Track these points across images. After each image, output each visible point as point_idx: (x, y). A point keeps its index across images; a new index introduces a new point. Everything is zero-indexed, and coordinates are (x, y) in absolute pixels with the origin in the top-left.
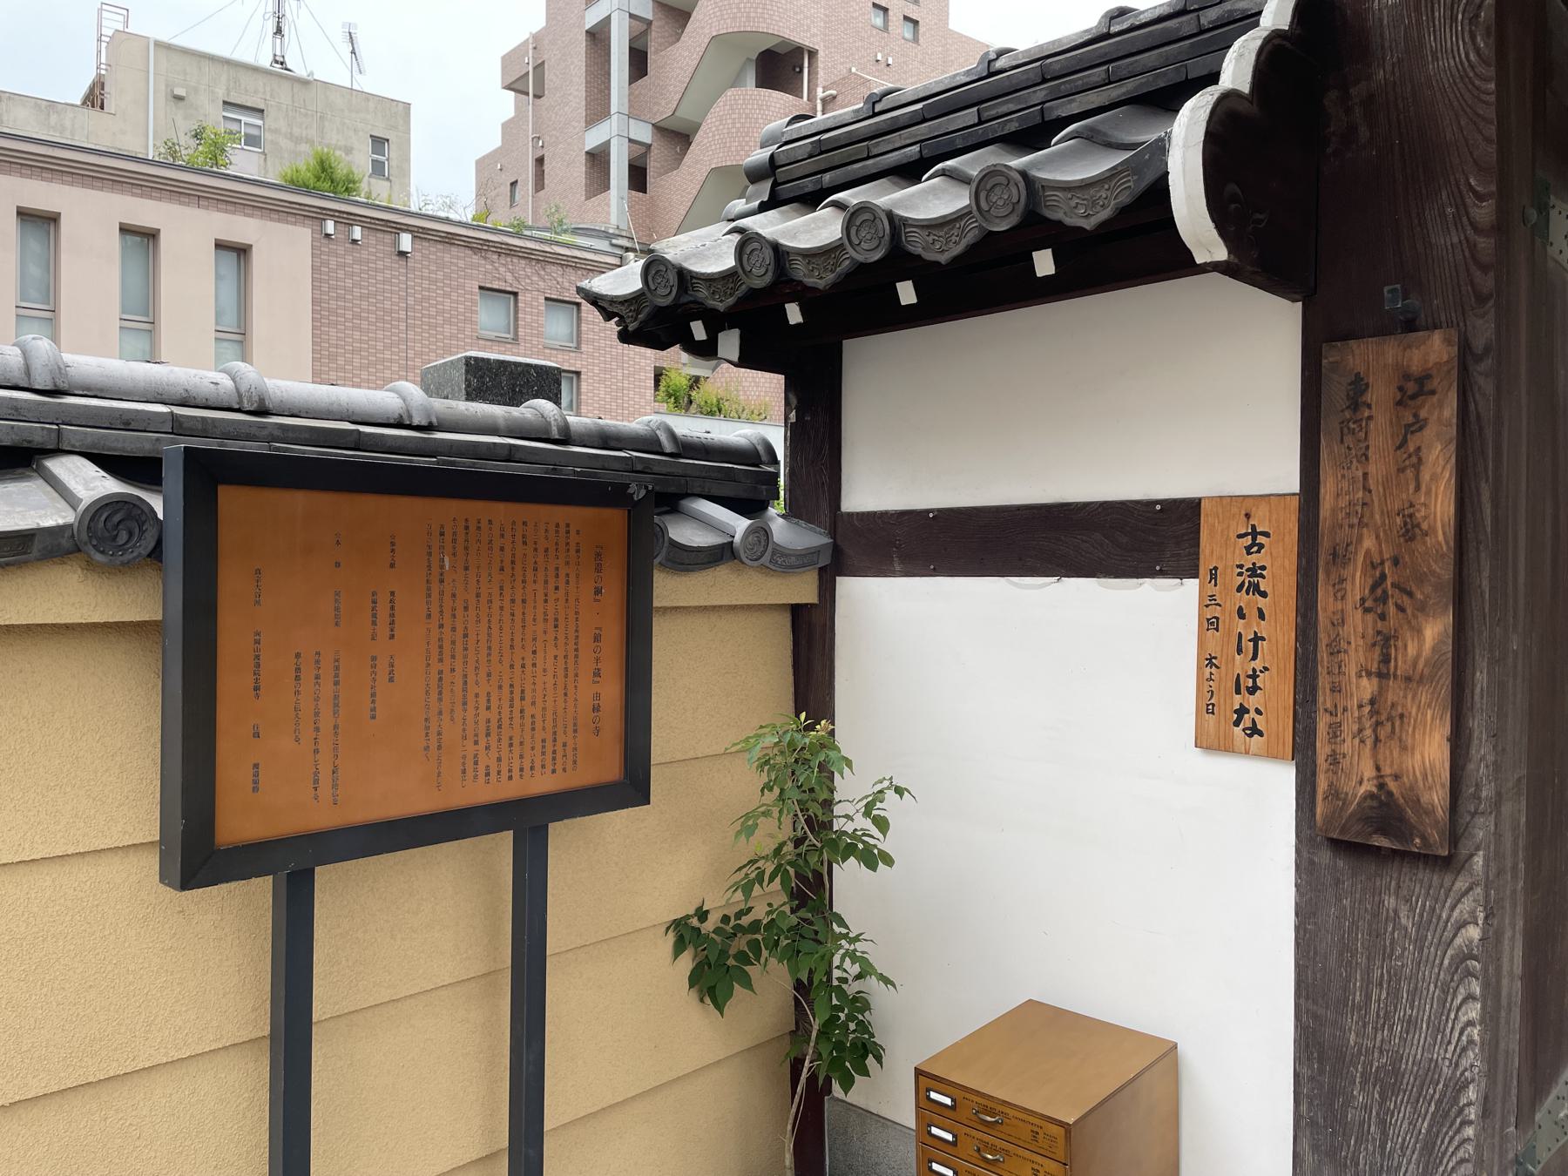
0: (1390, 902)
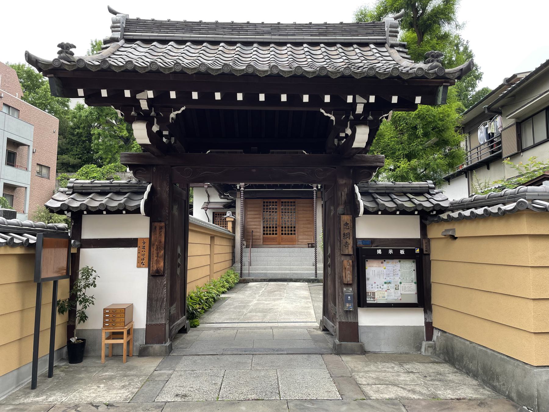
0: (157, 281)
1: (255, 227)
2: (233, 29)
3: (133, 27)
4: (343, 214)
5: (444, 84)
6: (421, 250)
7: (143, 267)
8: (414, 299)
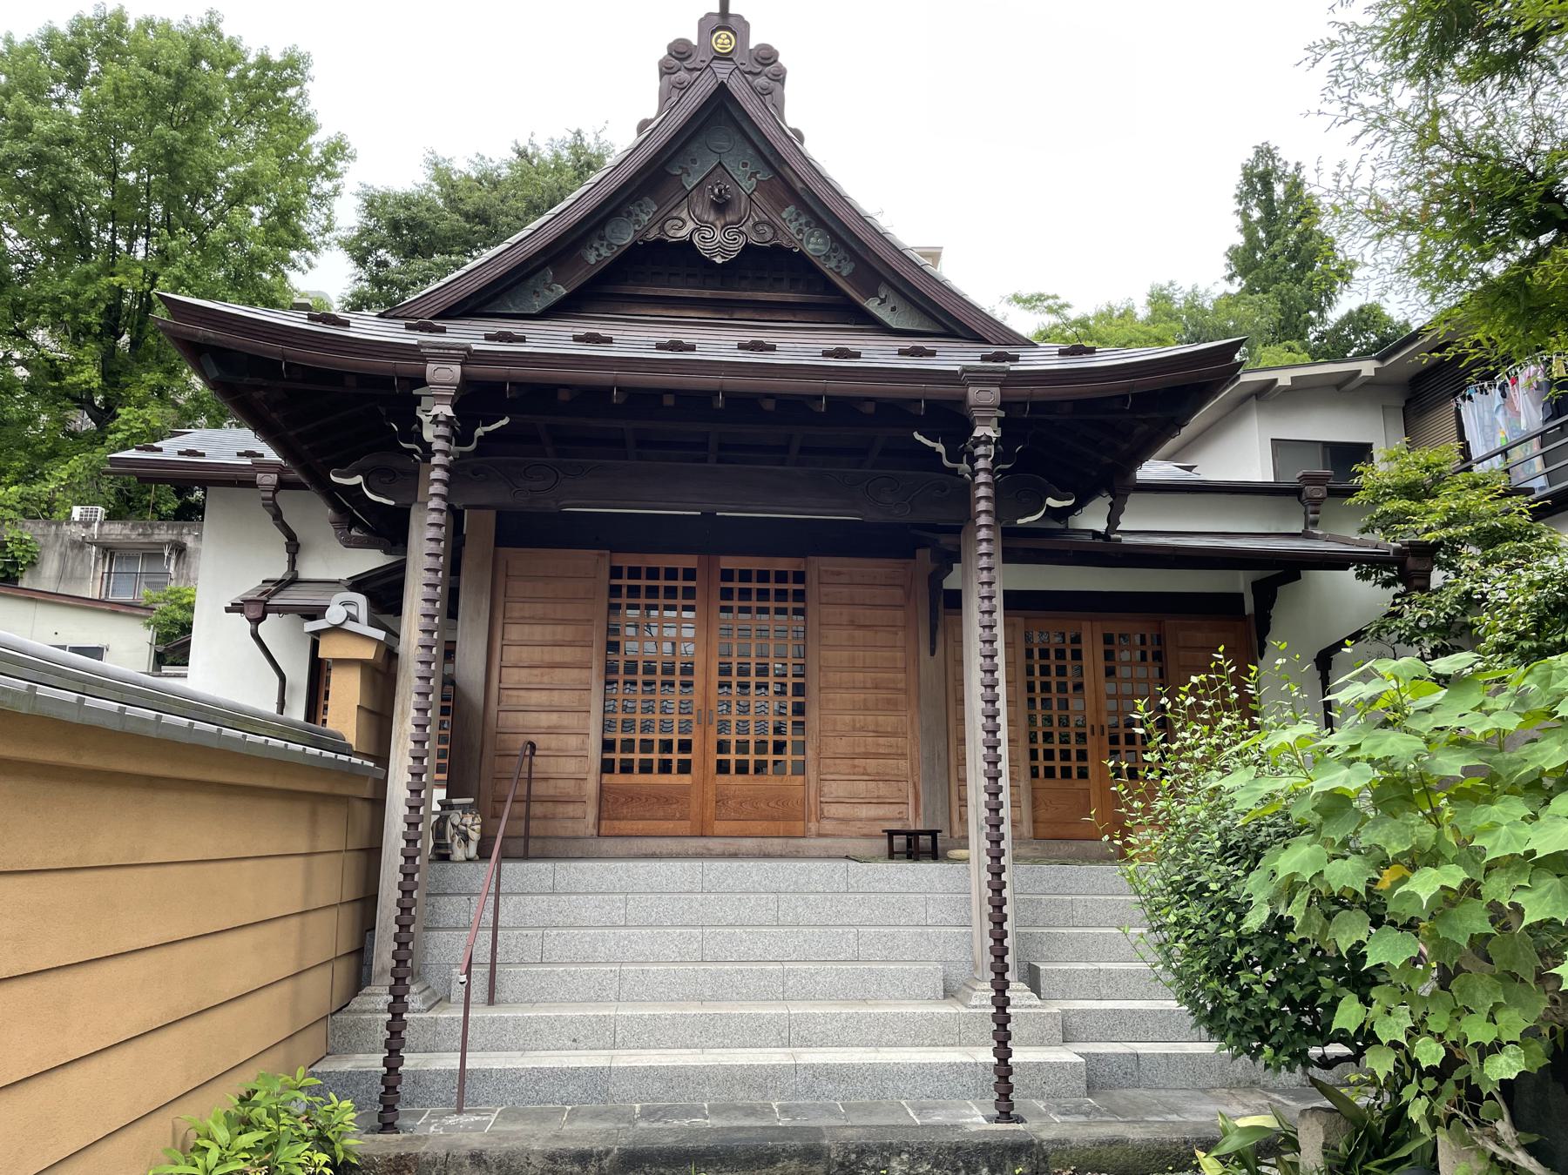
1: (546, 720)
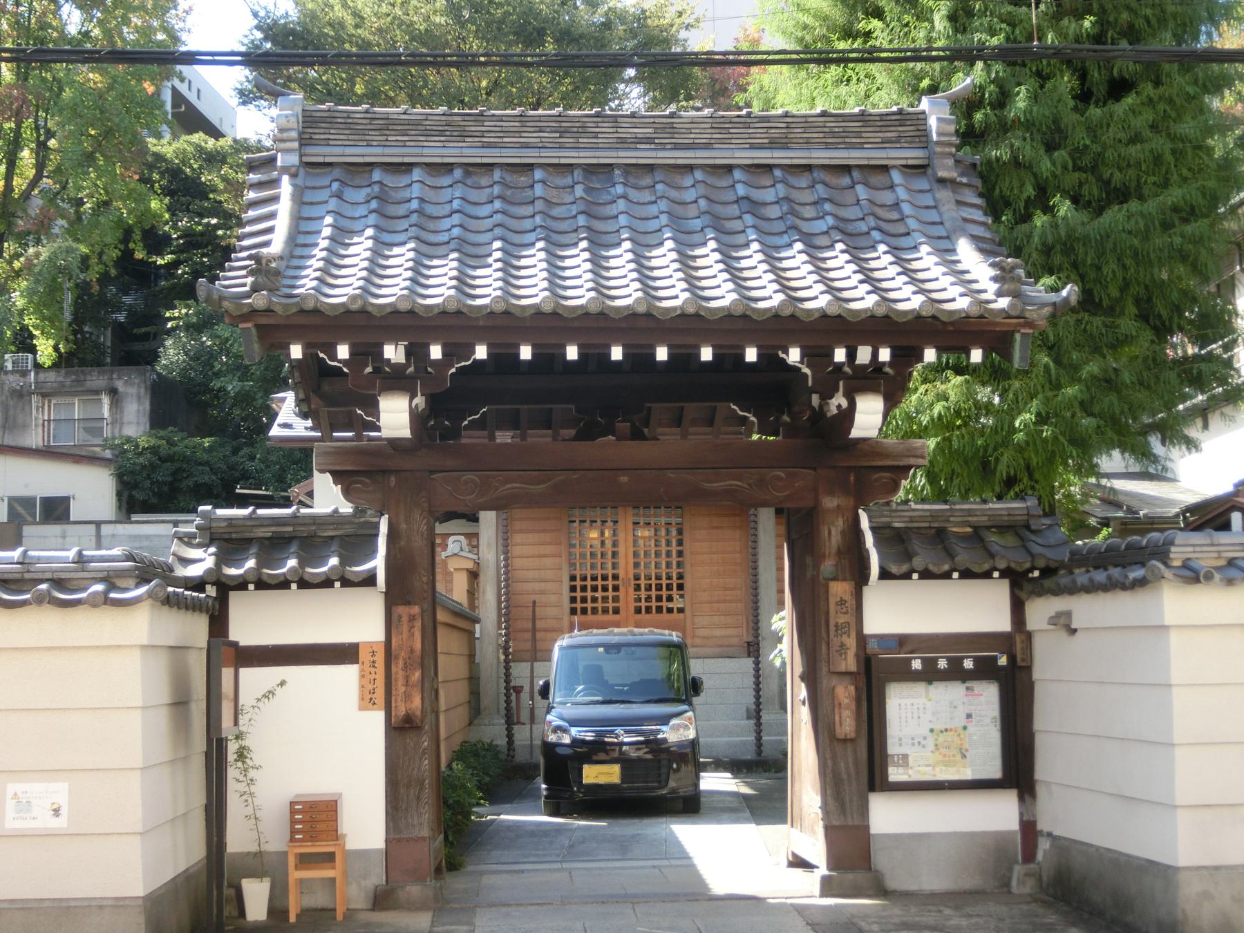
1: (538, 586)
2: (563, 132)
3: (322, 131)
4: (835, 579)
5: (1023, 331)
6: (1012, 658)
7: (372, 710)
8: (993, 769)
